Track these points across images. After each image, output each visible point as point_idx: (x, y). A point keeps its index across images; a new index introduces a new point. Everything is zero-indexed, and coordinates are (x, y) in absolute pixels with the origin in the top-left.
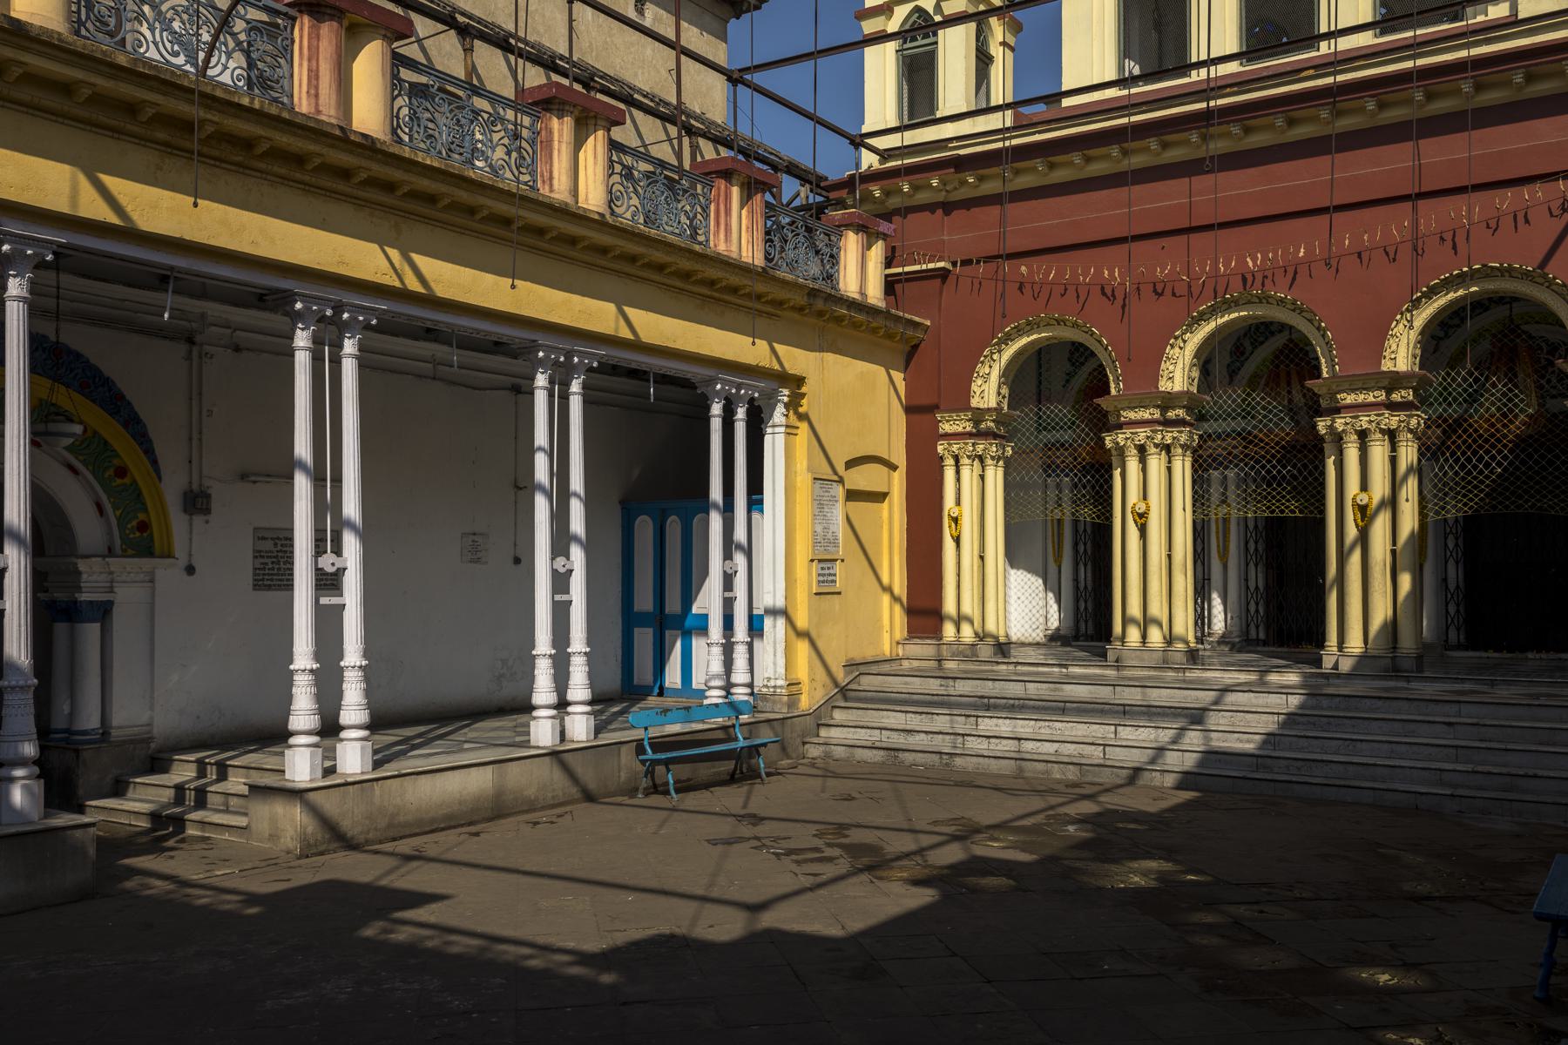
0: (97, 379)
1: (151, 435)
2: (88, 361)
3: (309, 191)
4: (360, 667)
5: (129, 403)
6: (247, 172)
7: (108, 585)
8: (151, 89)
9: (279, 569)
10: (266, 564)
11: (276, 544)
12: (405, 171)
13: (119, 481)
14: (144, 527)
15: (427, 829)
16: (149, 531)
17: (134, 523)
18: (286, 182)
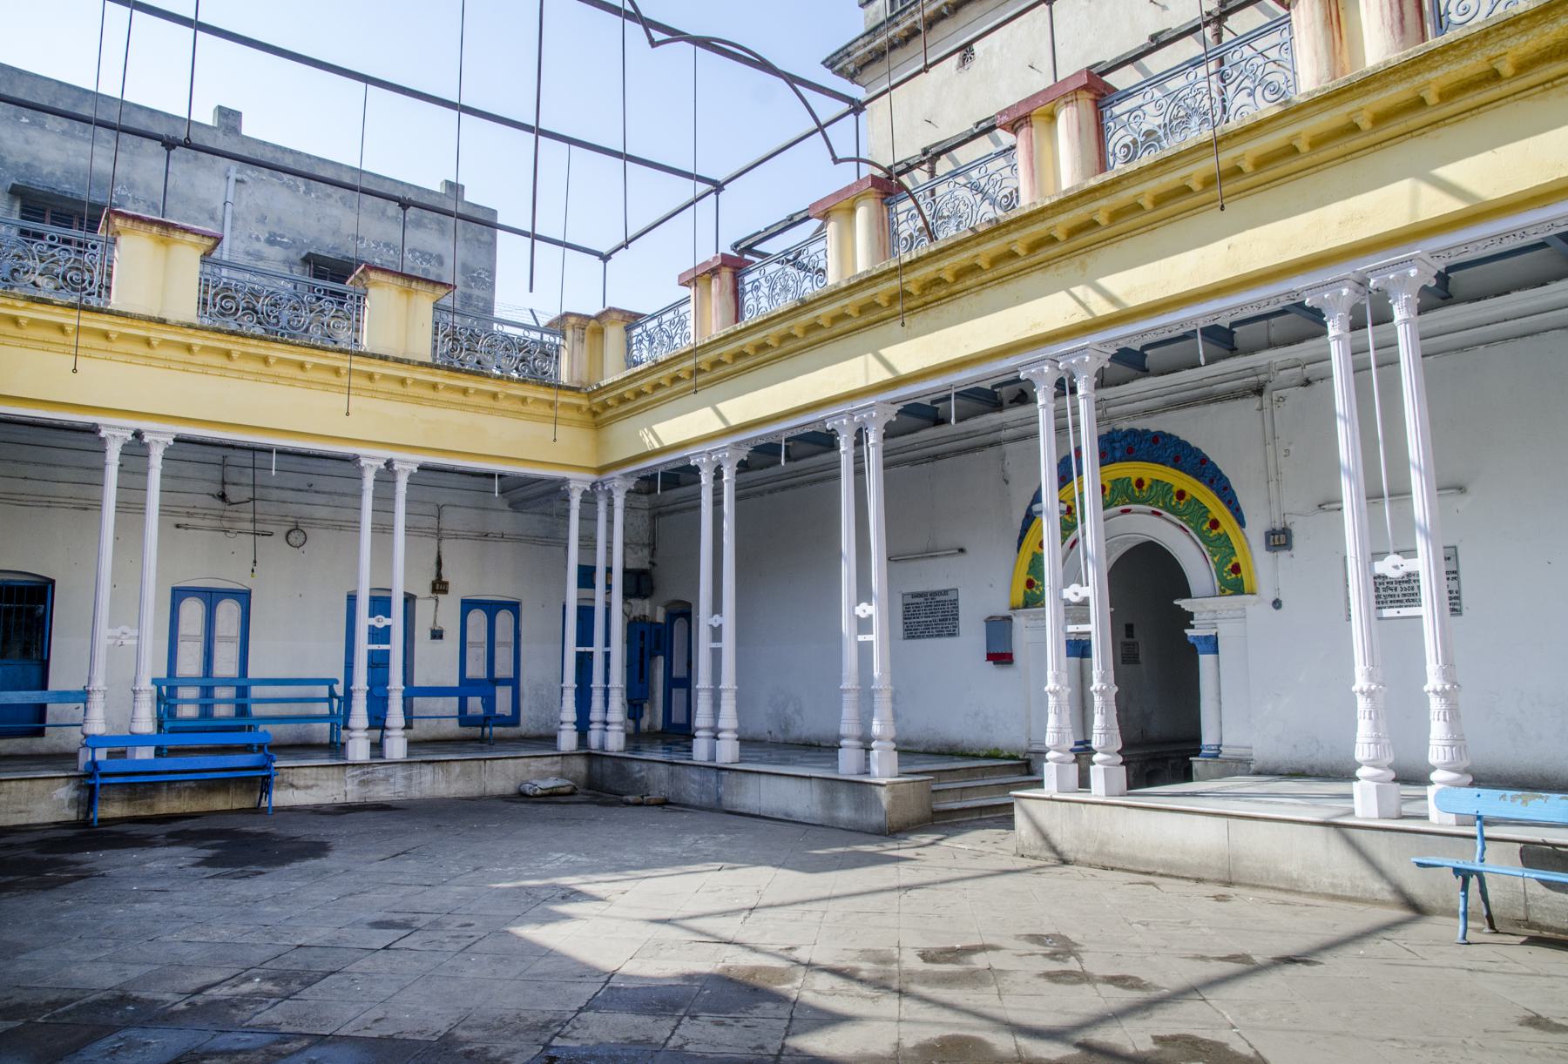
1: (1233, 486)
2: (1178, 438)
5: (1213, 464)
6: (958, 296)
12: (1043, 221)
13: (1214, 532)
14: (1236, 569)
15: (1143, 869)
17: (1230, 566)
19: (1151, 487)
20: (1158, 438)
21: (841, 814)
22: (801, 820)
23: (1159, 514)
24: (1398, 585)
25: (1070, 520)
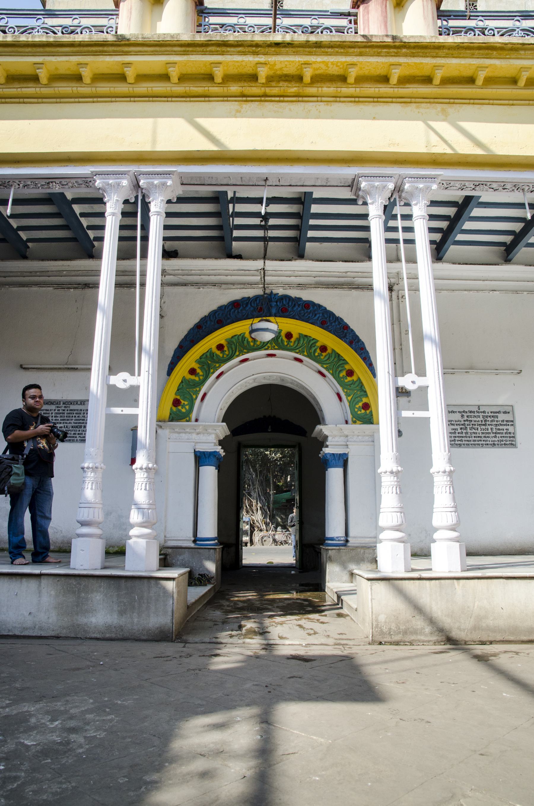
0: (331, 319)
2: (326, 308)
3: (359, 102)
4: (445, 472)
5: (352, 330)
7: (344, 443)
8: (212, 53)
9: (467, 433)
10: (457, 429)
11: (462, 416)
12: (433, 57)
13: (349, 379)
14: (366, 406)
15: (525, 638)
16: (370, 409)
17: (360, 404)
18: (338, 99)
19: (298, 340)
20: (308, 305)
21: (93, 620)
22: (17, 633)
23: (300, 361)
24: (478, 427)
25: (221, 355)
